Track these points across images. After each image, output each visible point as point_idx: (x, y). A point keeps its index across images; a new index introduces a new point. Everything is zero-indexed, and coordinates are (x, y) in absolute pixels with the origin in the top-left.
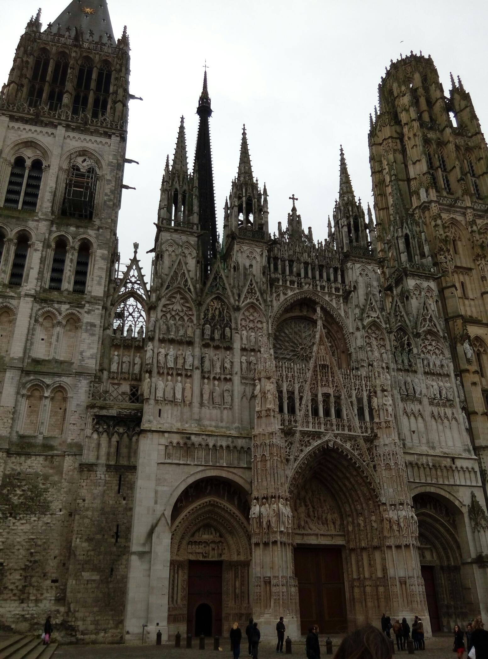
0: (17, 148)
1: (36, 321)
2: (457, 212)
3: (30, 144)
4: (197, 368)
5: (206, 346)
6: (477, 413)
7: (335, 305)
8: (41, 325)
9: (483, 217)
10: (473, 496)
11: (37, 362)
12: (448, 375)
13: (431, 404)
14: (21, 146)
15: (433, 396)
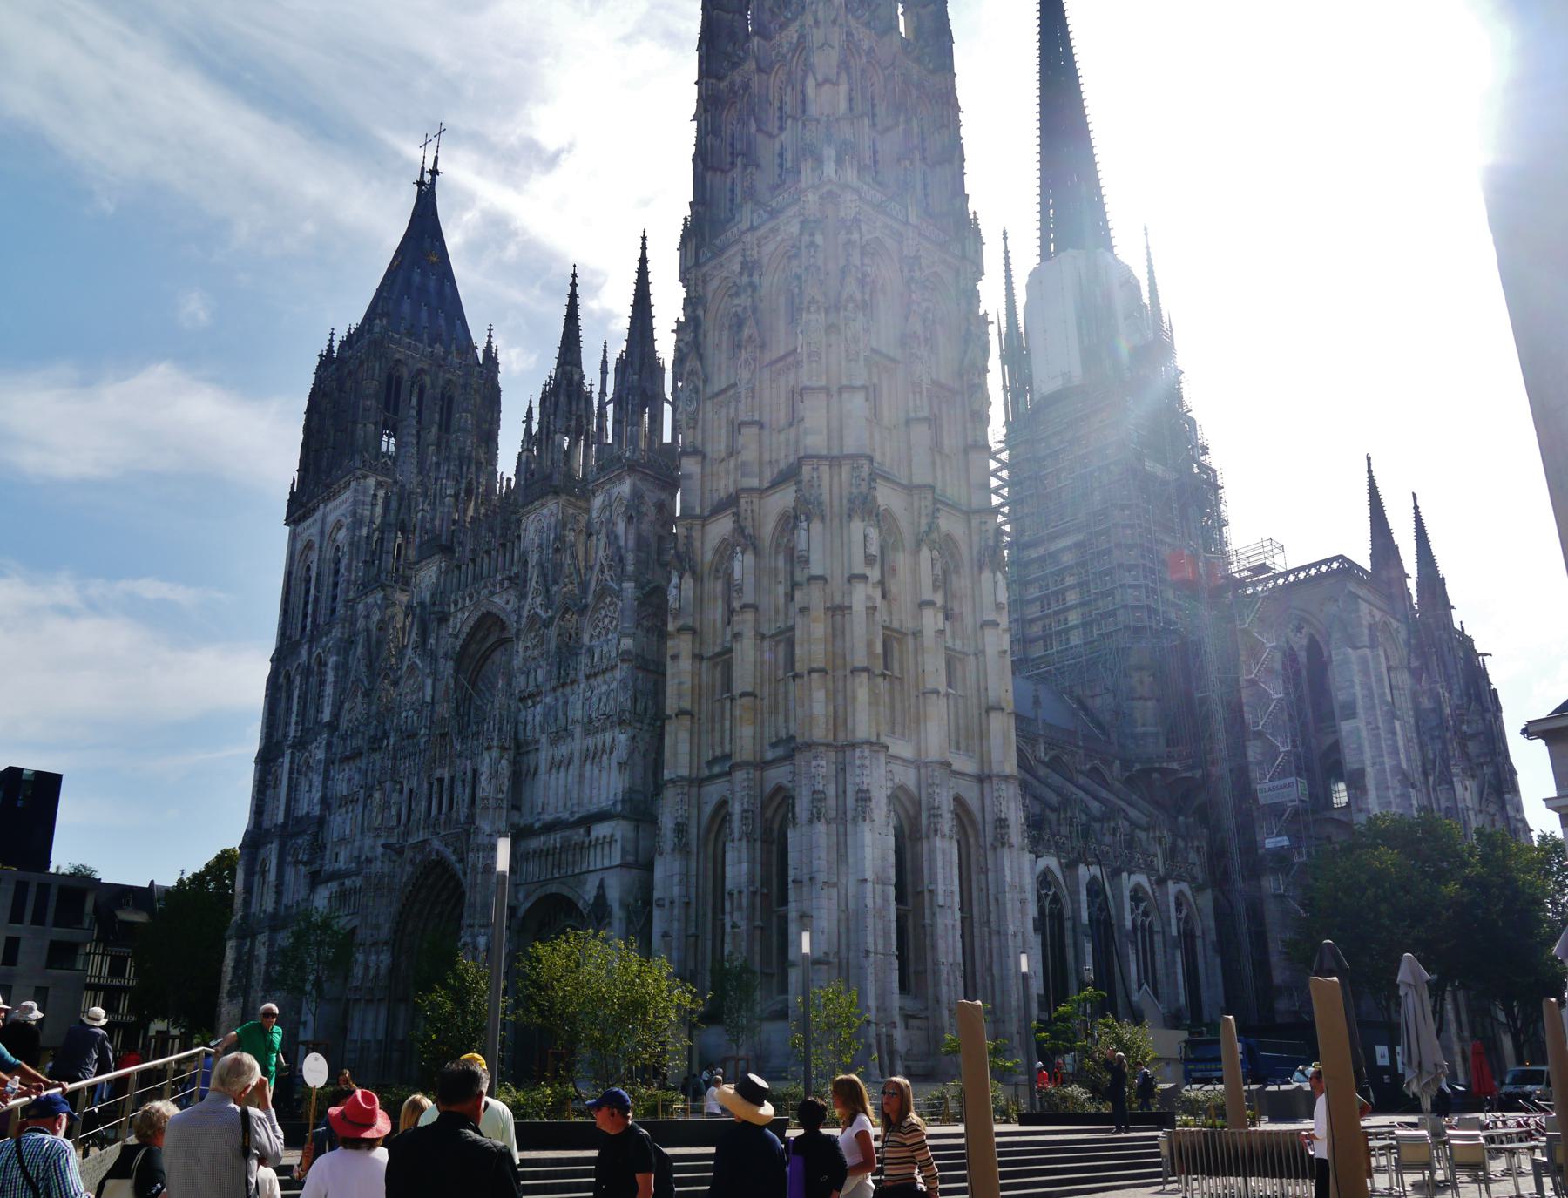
0: (304, 557)
1: (299, 772)
2: (734, 255)
3: (309, 546)
4: (361, 787)
5: (374, 750)
6: (670, 717)
7: (509, 607)
8: (306, 776)
9: (777, 230)
10: (601, 886)
11: (299, 820)
12: (617, 665)
13: (587, 733)
14: (306, 552)
15: (586, 719)
